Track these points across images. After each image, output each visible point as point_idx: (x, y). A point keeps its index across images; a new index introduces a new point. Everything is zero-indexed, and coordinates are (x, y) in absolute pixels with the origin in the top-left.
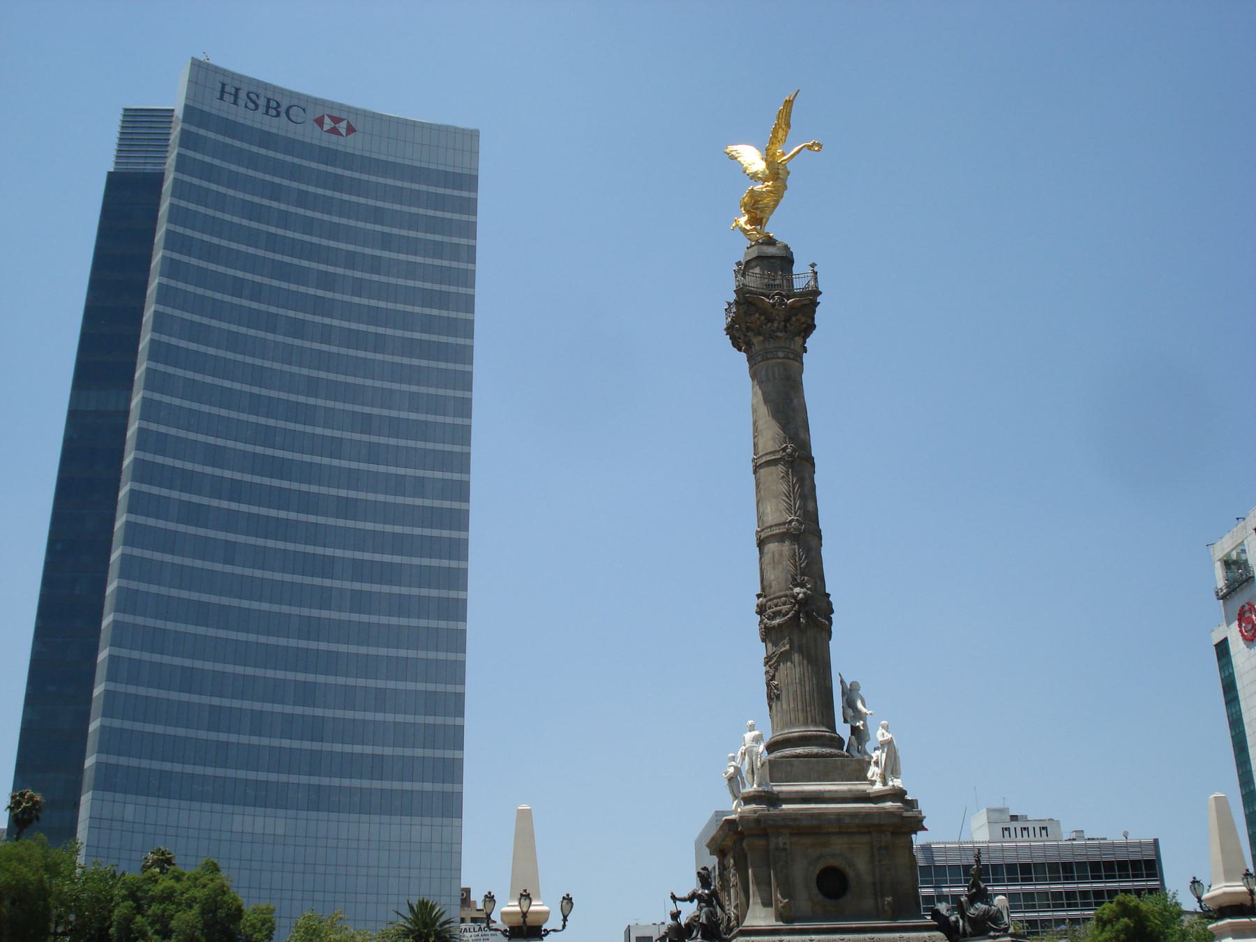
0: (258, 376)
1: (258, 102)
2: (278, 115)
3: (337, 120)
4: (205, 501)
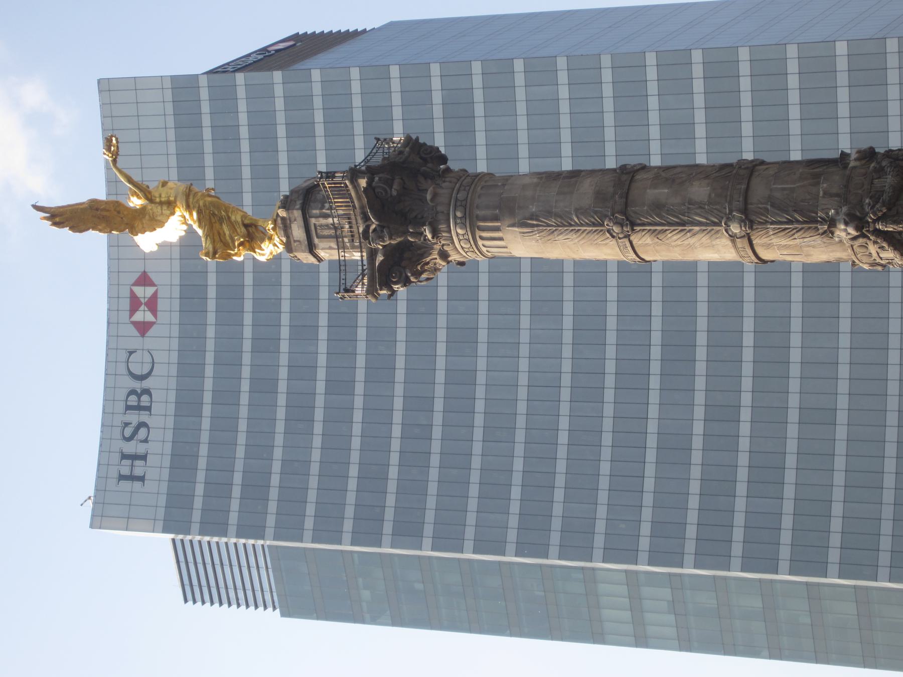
1: (135, 423)
2: (147, 392)
3: (135, 304)
4: (743, 459)
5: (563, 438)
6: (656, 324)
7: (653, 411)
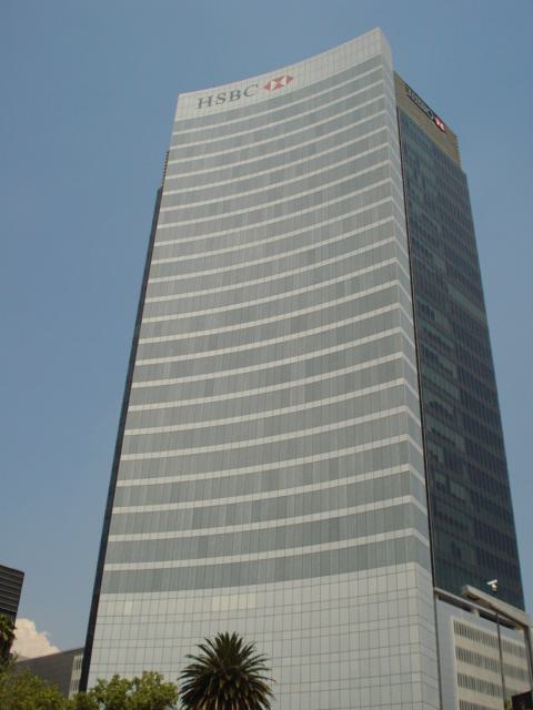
2: (239, 97)
5: (206, 273)
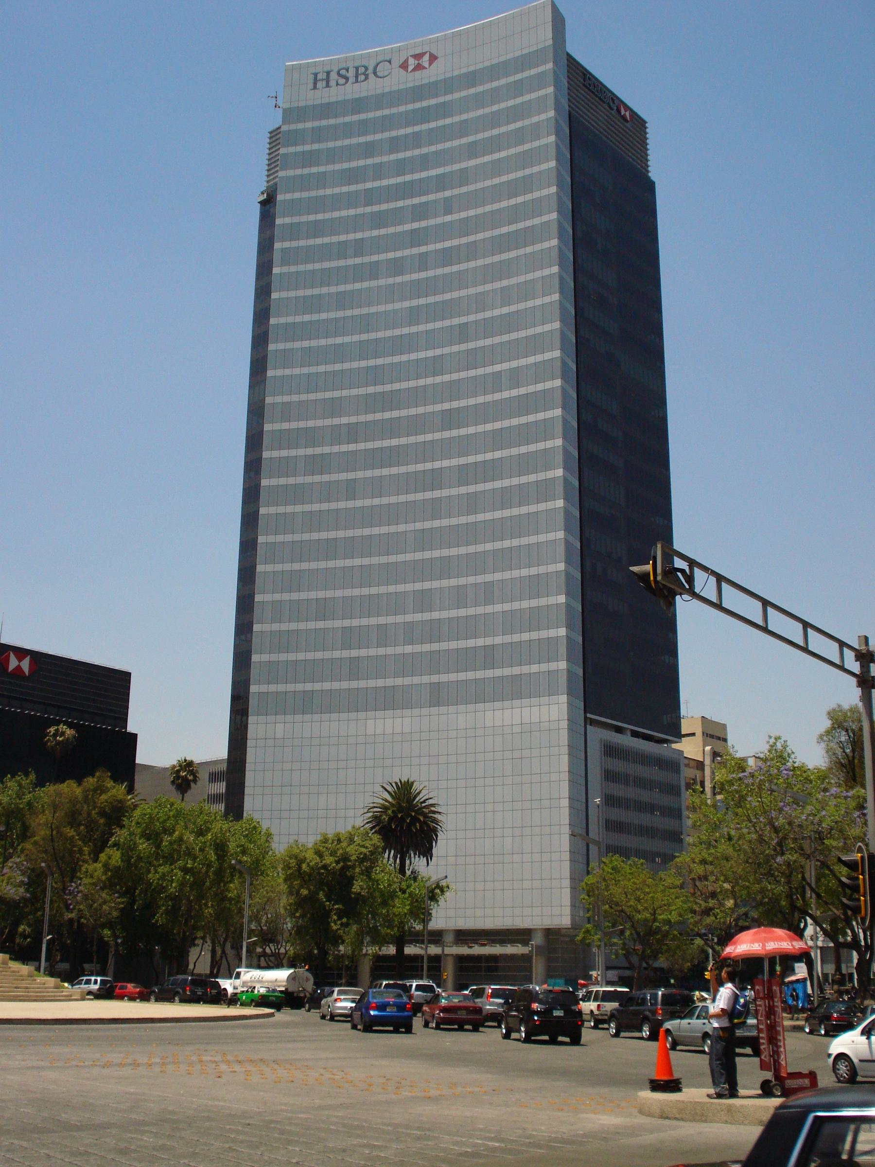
0: (366, 323)
1: (348, 75)
2: (367, 78)
3: (418, 57)
5: (339, 340)
6: (404, 385)
7: (354, 392)
